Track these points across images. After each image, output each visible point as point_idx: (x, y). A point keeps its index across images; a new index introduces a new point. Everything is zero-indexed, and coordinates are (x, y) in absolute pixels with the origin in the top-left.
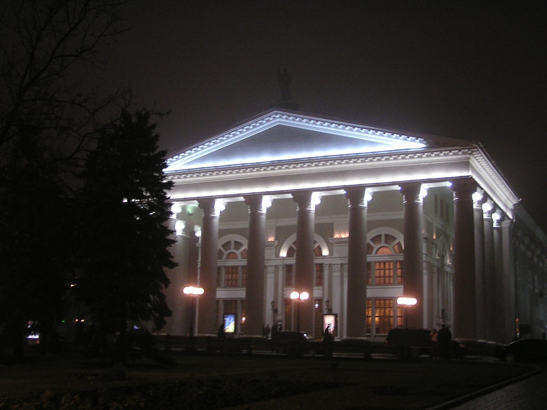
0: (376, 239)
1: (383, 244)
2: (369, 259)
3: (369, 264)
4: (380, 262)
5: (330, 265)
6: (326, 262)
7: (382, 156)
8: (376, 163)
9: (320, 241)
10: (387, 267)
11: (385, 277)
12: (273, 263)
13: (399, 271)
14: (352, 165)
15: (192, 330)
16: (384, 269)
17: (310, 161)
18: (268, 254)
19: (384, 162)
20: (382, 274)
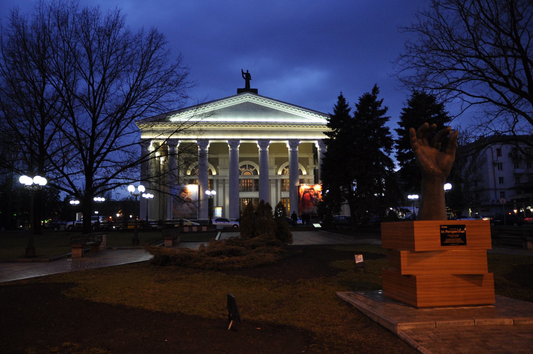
0: (244, 166)
1: (247, 170)
2: (240, 177)
3: (240, 180)
4: (244, 179)
5: (217, 180)
6: (215, 178)
7: (297, 124)
8: (305, 128)
9: (301, 167)
10: (248, 182)
11: (247, 187)
12: (275, 178)
13: (288, 185)
14: (292, 128)
15: (165, 212)
16: (247, 183)
17: (267, 123)
18: (271, 173)
19: (309, 128)
20: (246, 186)
